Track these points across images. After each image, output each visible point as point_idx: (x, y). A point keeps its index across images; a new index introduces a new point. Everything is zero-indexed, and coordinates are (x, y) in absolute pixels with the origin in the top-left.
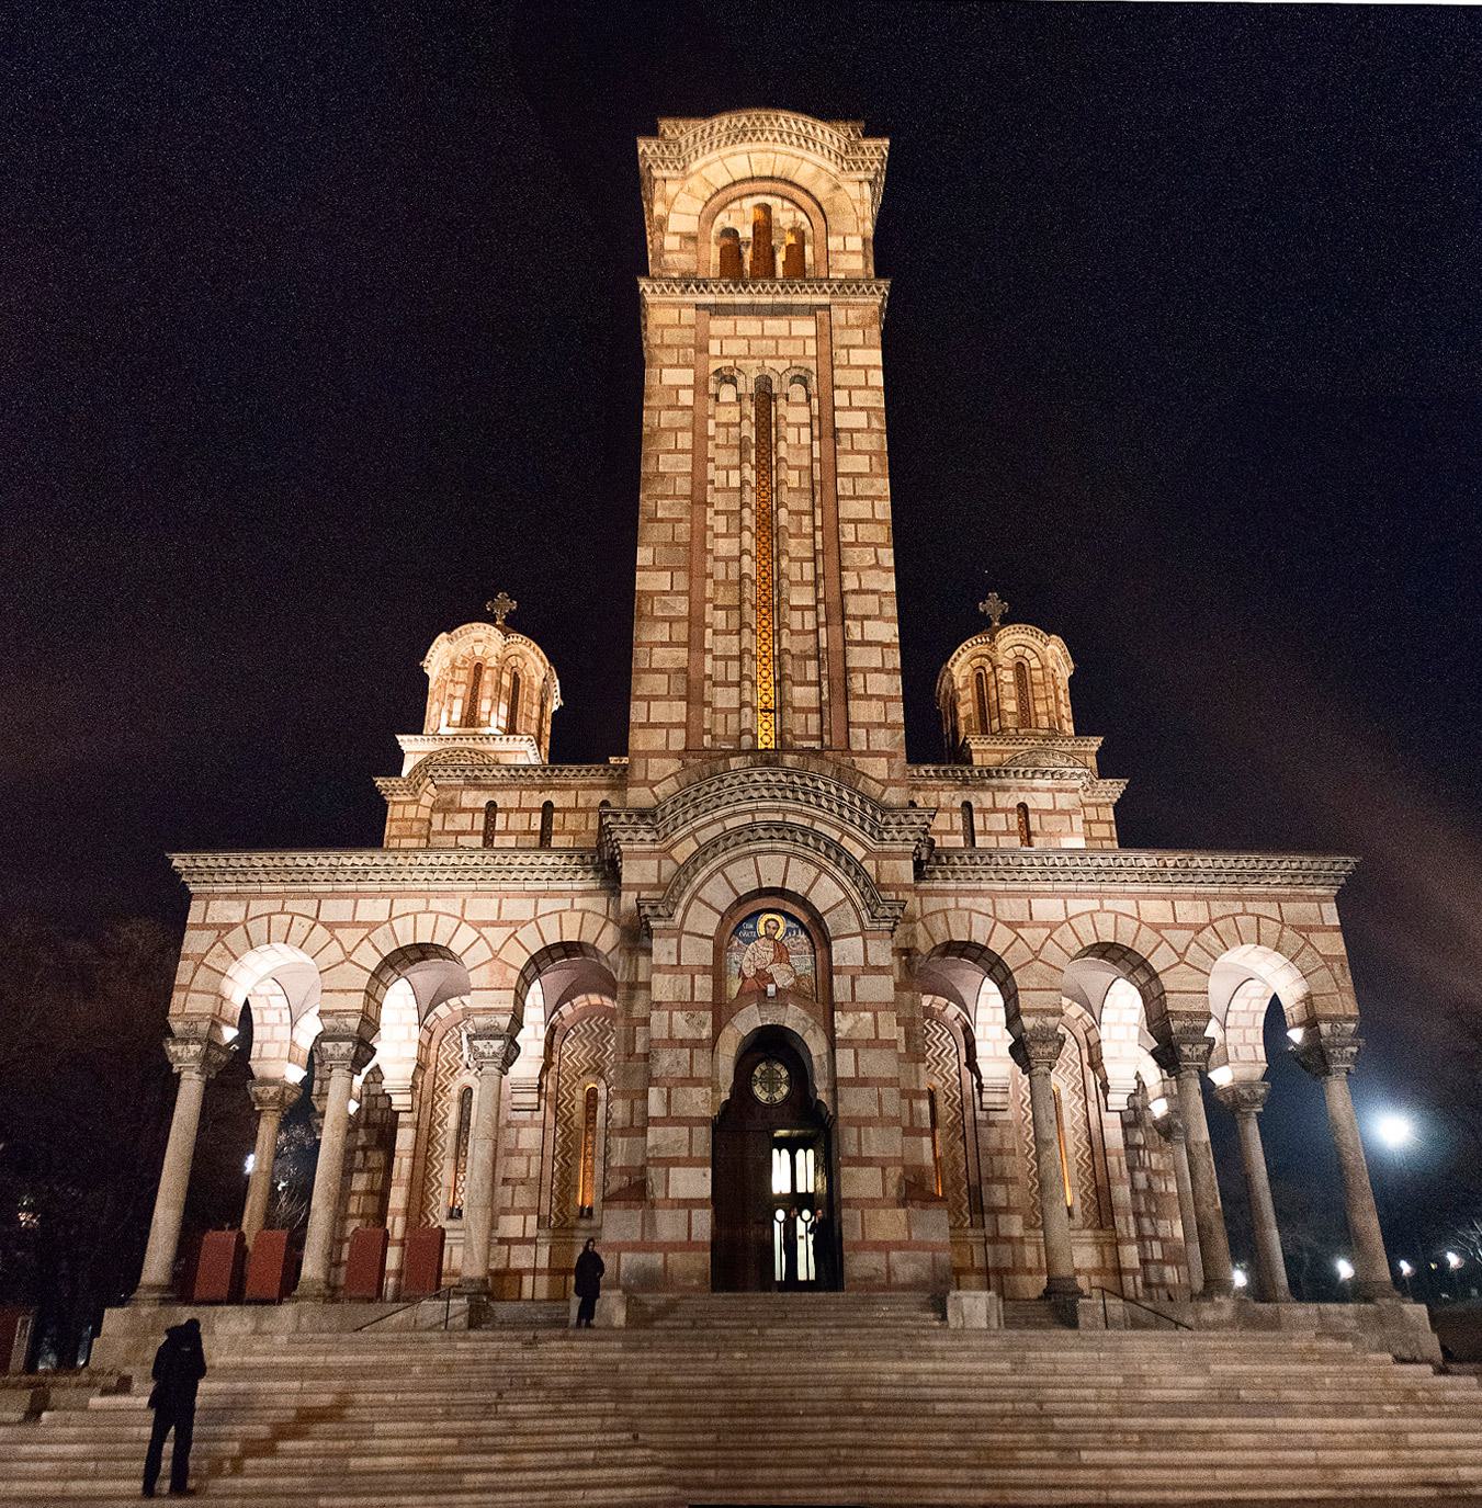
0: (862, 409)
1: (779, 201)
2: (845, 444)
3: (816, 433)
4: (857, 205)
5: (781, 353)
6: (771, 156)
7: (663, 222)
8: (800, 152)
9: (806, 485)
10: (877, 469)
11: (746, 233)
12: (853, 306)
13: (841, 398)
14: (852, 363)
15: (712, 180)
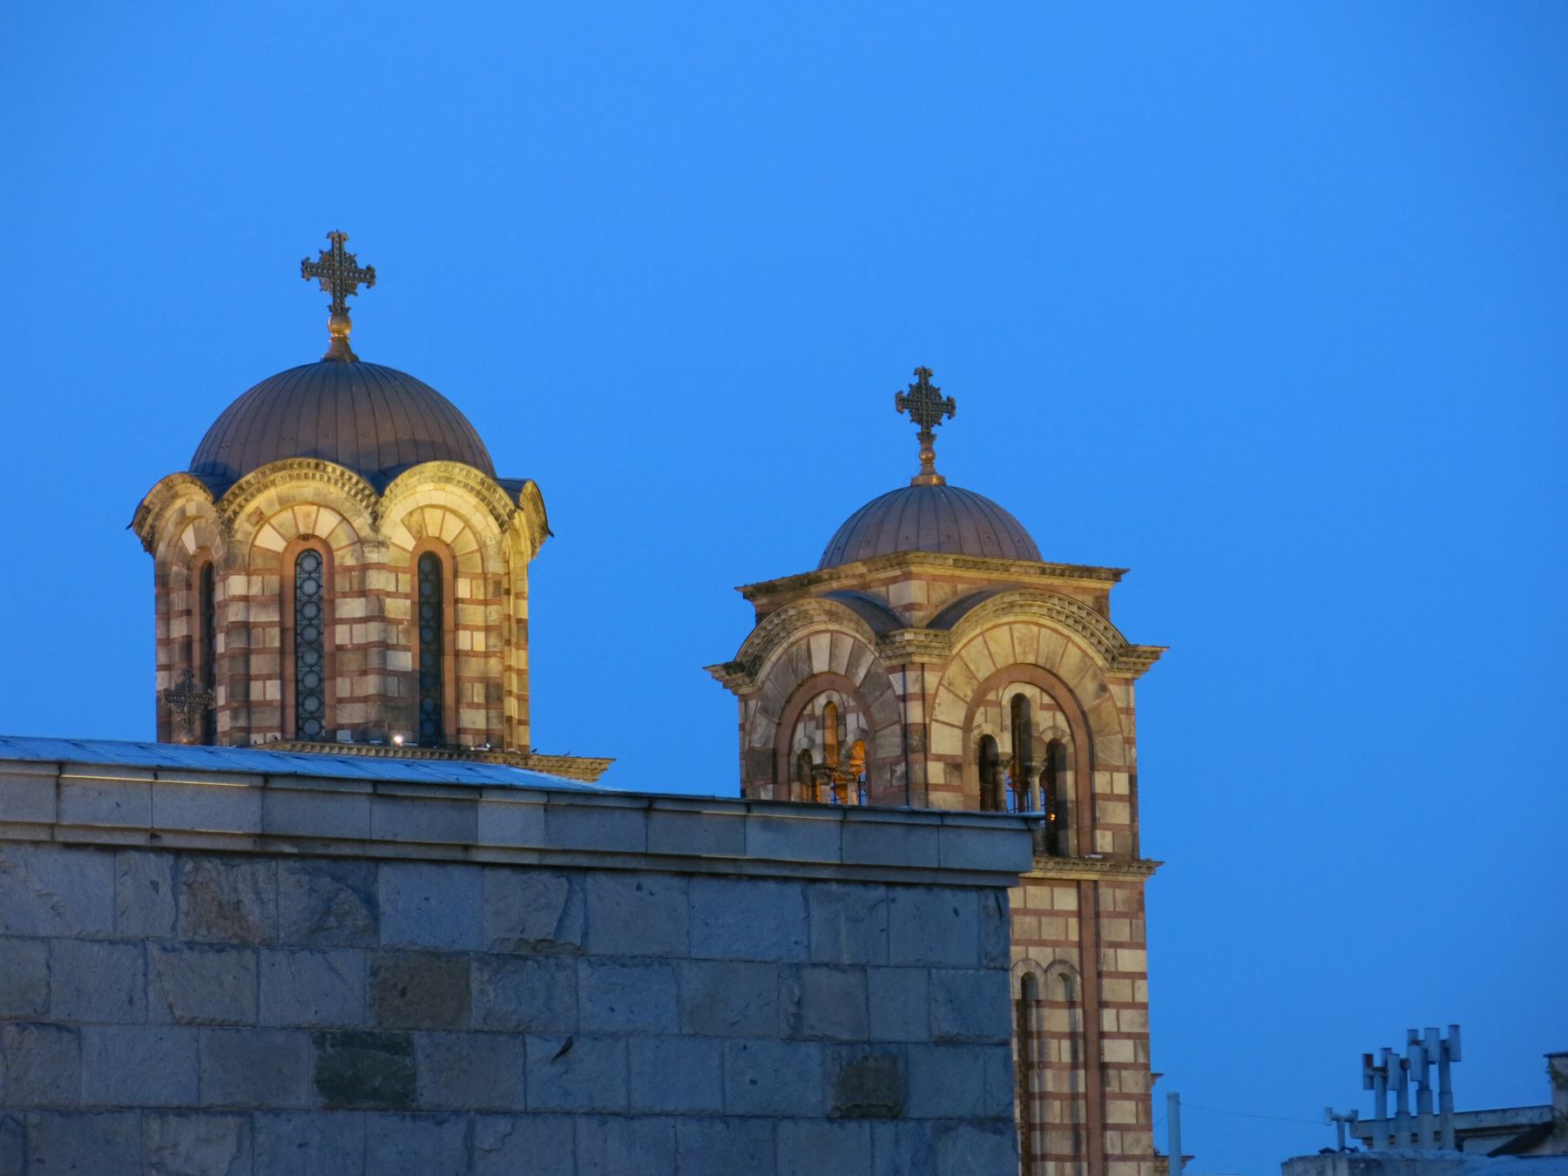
0: (1129, 1036)
1: (1037, 691)
2: (1113, 1087)
3: (1081, 1056)
4: (1123, 717)
5: (1045, 937)
6: (1035, 629)
7: (925, 729)
8: (1066, 631)
9: (1067, 1121)
10: (1143, 1121)
11: (1004, 745)
12: (1120, 885)
13: (1109, 1020)
14: (1121, 969)
15: (972, 667)
